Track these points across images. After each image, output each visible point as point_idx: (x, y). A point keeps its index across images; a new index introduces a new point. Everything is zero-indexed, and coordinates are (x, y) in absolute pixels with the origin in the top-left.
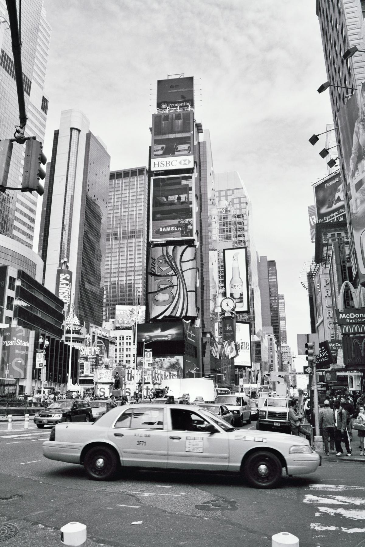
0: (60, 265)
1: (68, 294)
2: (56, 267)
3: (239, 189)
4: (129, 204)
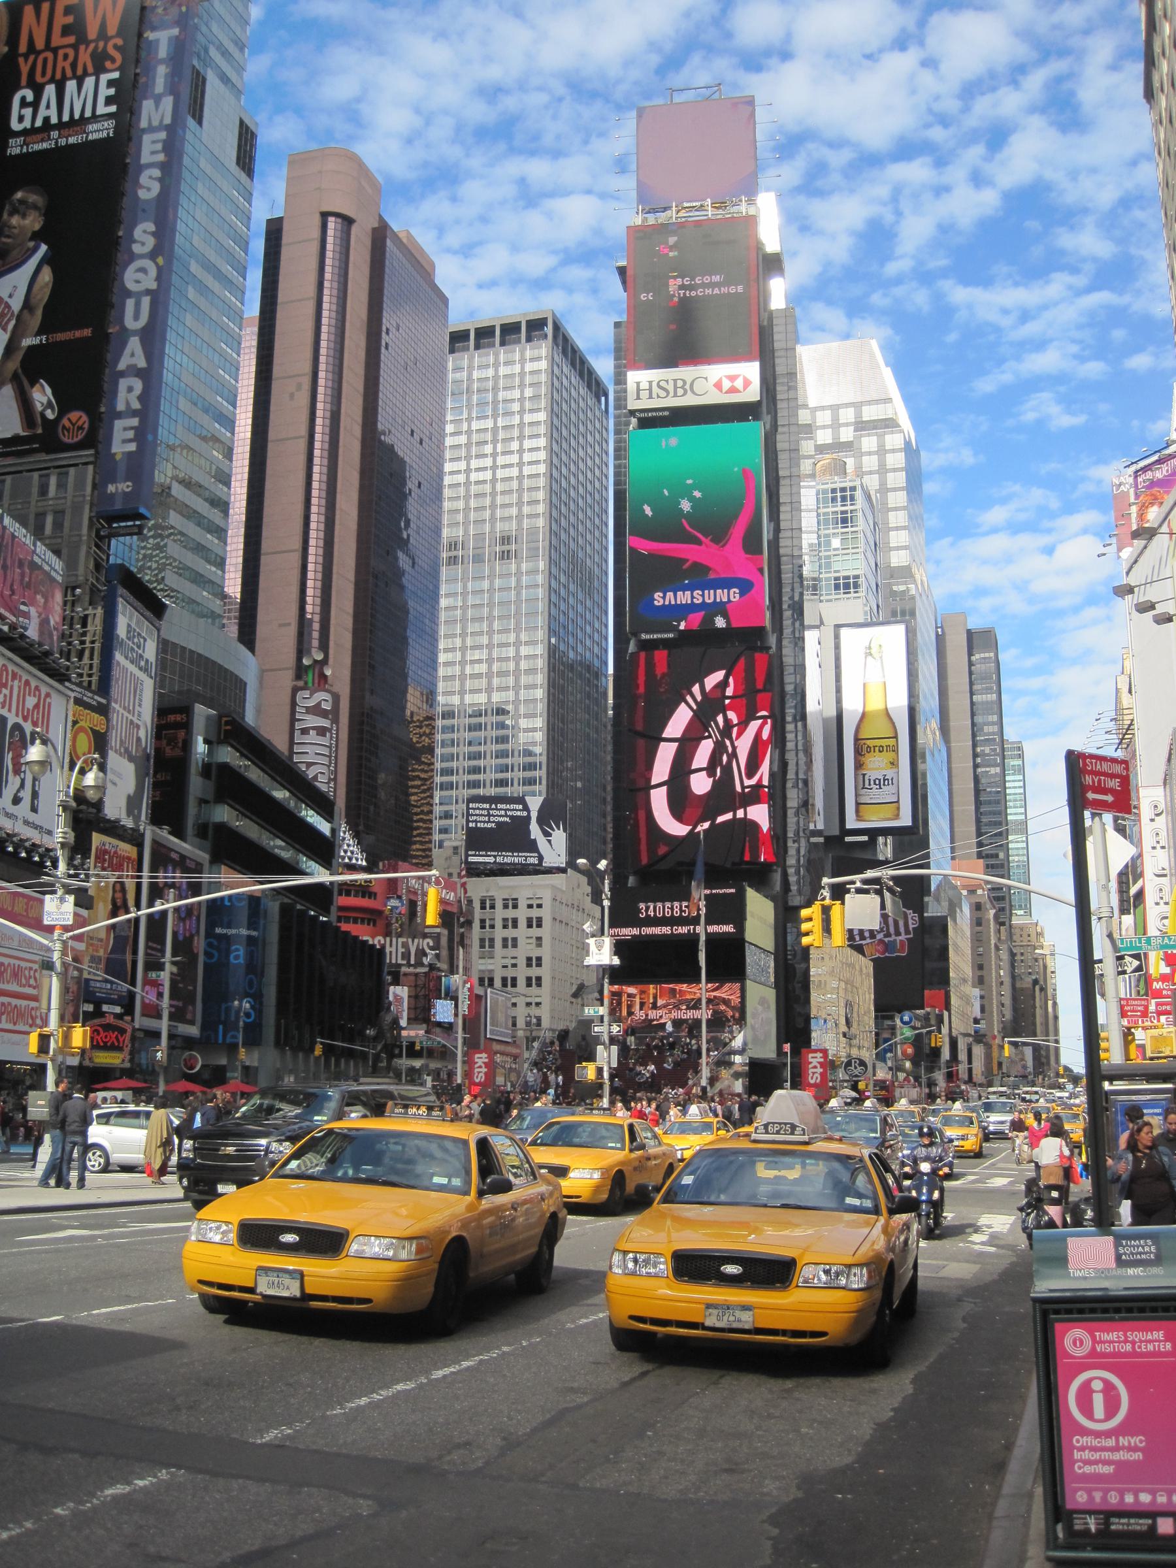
0: (300, 671)
3: (877, 402)
4: (495, 442)
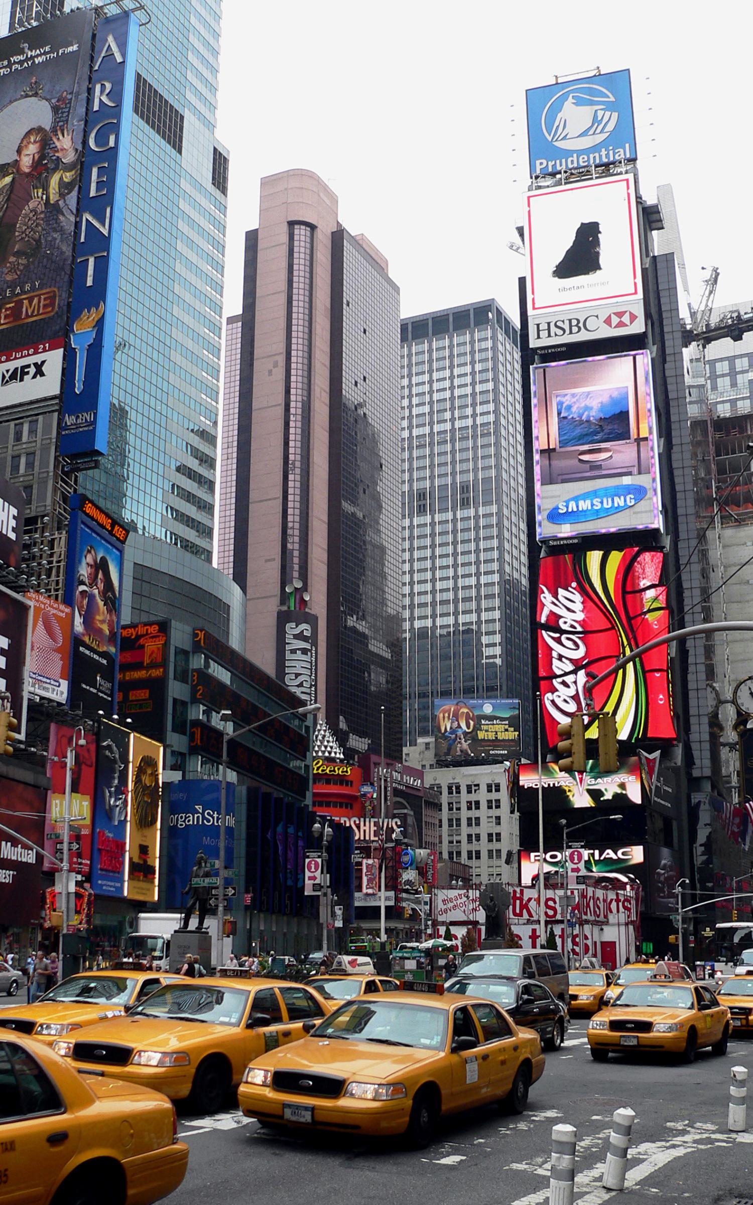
0: (284, 598)
1: (305, 674)
2: (273, 606)
4: (452, 409)
